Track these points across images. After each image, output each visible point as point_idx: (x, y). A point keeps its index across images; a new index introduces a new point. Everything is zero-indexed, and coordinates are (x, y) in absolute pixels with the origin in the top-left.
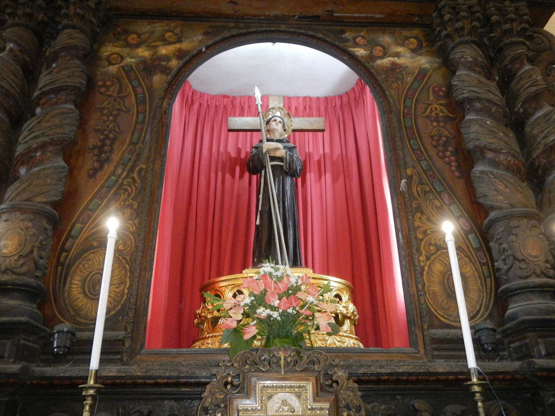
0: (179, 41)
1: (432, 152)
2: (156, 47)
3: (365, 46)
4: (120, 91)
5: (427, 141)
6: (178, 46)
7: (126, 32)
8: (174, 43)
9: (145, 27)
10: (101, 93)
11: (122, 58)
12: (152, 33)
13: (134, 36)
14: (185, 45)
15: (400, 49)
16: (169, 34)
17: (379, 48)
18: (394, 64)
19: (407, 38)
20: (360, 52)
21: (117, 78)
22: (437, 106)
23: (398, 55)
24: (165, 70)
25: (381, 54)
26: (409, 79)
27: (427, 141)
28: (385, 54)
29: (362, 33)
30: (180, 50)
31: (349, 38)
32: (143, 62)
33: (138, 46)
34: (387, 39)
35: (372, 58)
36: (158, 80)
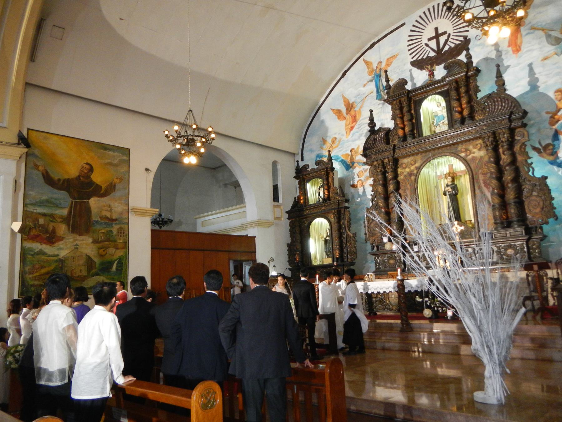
0: (415, 163)
1: (483, 185)
2: (410, 167)
3: (464, 152)
4: (405, 184)
5: (482, 182)
6: (415, 166)
7: (402, 164)
8: (414, 165)
9: (406, 161)
10: (402, 185)
11: (403, 173)
12: (408, 162)
13: (404, 165)
14: (417, 165)
15: (475, 150)
16: (412, 162)
17: (468, 151)
18: (473, 157)
19: (477, 145)
20: (463, 155)
21: (404, 180)
22: (485, 169)
23: (474, 153)
24: (413, 174)
25: (469, 154)
26: (477, 161)
27: (482, 182)
28: (470, 153)
29: (463, 147)
30: (416, 167)
31: (460, 150)
32: (408, 173)
33: (406, 168)
34: (471, 147)
35: (467, 156)
36: (413, 178)
